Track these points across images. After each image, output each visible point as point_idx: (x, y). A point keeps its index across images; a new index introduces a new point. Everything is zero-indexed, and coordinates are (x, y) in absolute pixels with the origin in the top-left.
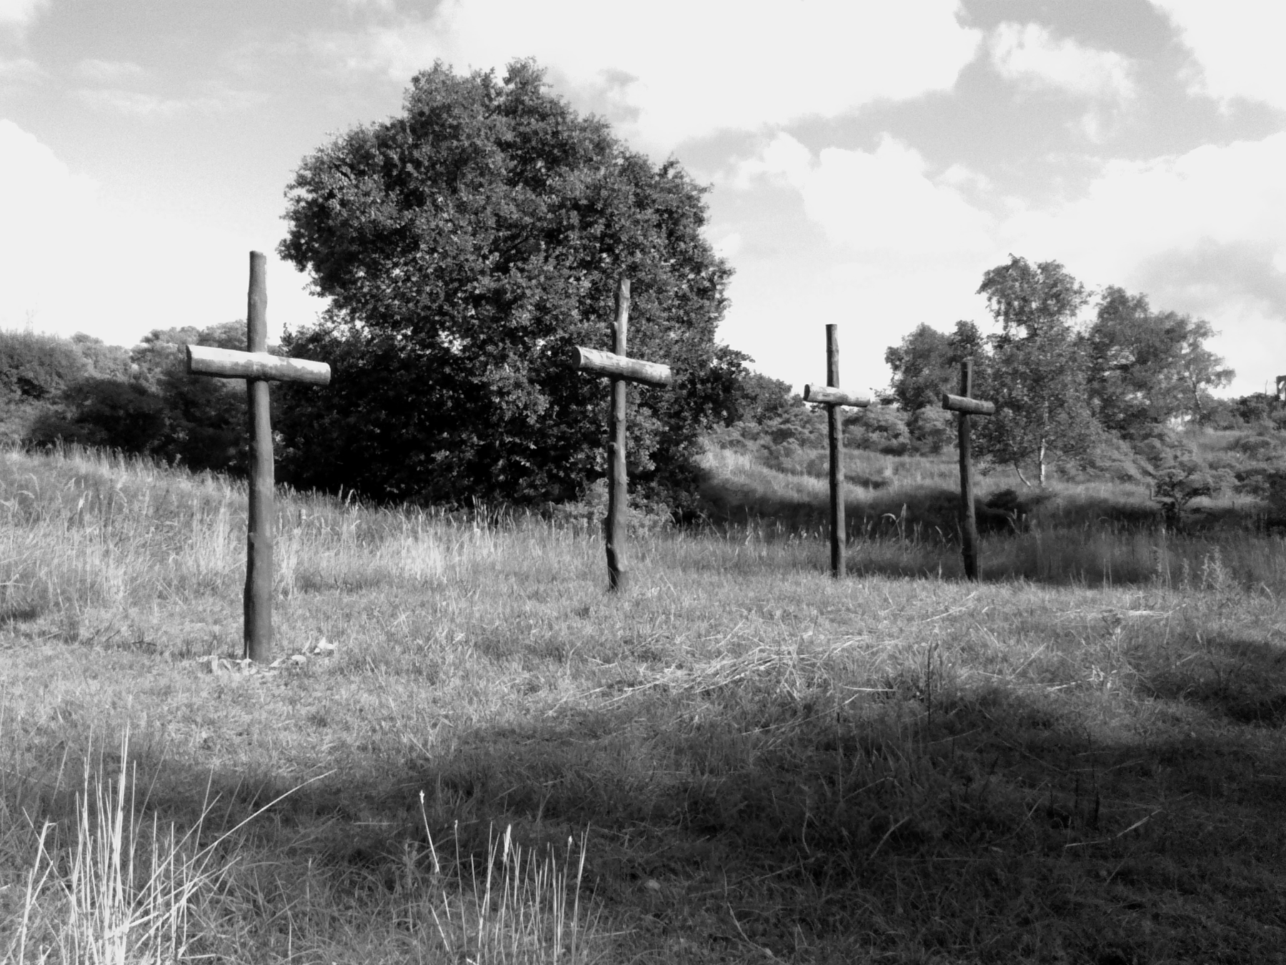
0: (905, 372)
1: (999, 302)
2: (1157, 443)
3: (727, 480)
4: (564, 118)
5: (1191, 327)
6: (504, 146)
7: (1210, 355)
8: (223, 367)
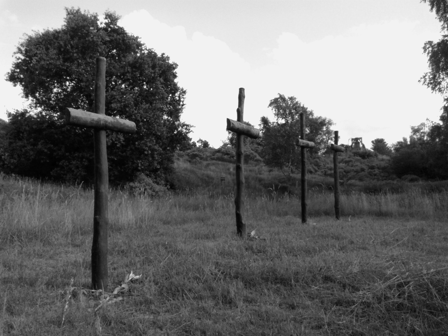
1: (275, 111)
2: (318, 160)
5: (327, 121)
6: (105, 43)
8: (87, 121)
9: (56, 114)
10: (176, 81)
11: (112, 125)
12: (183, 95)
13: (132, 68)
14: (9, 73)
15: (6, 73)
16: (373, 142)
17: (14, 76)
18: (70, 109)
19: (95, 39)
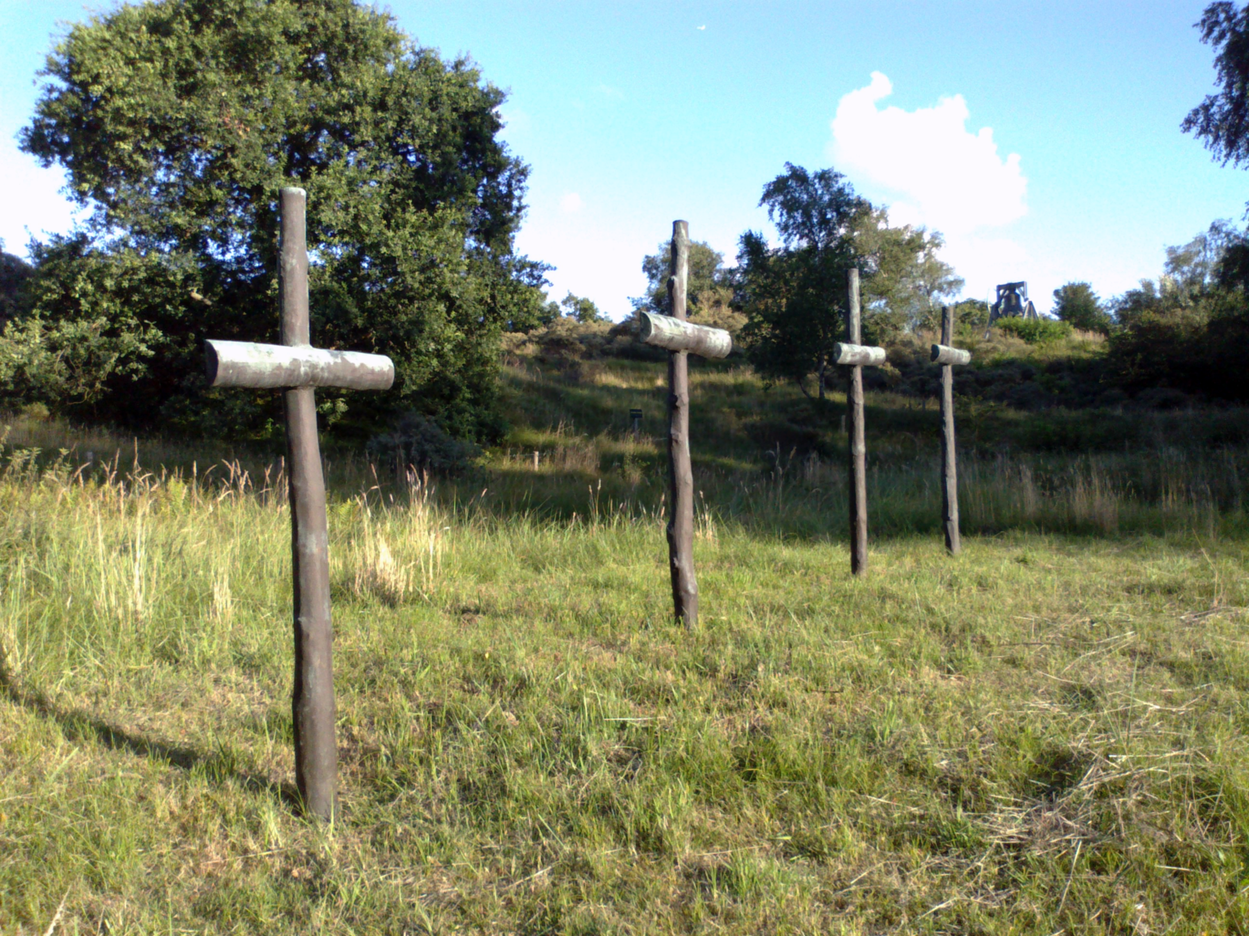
0: (661, 281)
3: (1144, 558)
4: (355, 11)
5: (926, 238)
6: (293, 38)
7: (942, 265)
8: (261, 373)
9: (166, 242)
10: (498, 137)
11: (329, 372)
12: (519, 181)
13: (375, 110)
14: (26, 129)
15: (19, 129)
16: (1056, 293)
17: (42, 137)
18: (217, 345)
19: (262, 29)
